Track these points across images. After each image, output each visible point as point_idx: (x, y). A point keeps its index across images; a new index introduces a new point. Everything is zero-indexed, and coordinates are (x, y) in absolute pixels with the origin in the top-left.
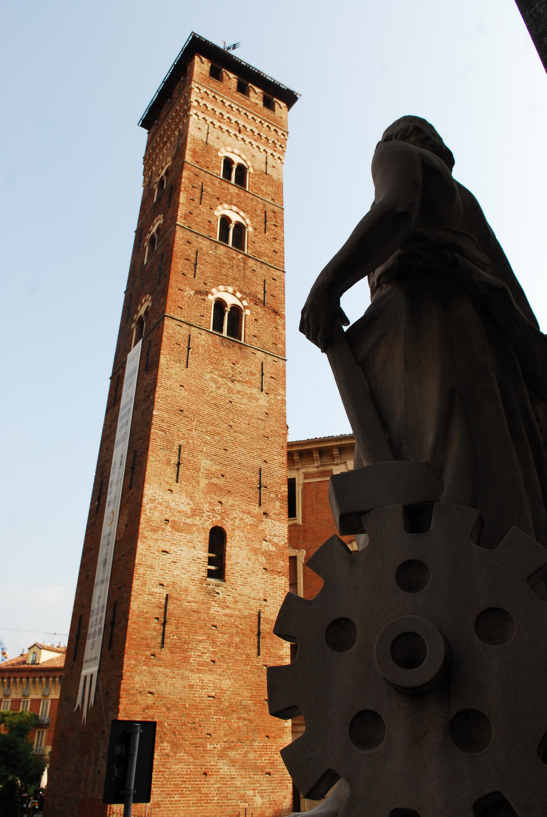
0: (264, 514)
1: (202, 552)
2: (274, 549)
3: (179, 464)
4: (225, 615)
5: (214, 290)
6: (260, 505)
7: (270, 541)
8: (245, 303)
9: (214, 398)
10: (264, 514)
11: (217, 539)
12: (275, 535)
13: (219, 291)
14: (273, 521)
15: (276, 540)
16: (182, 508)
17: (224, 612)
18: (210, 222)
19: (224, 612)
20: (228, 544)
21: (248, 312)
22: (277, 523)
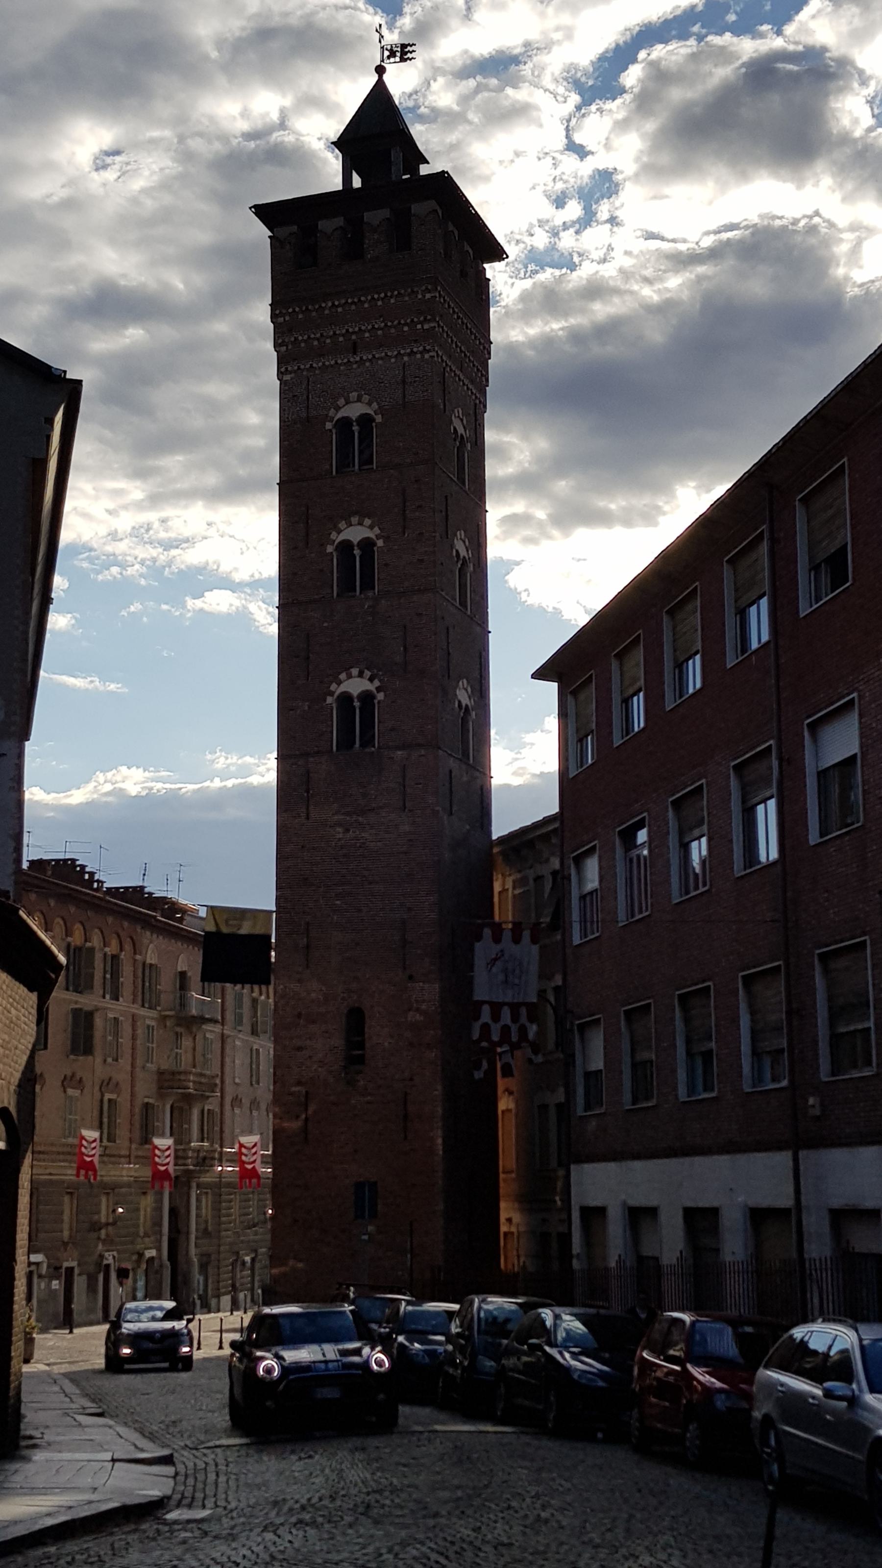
0: (411, 977)
1: (338, 1041)
2: (422, 1018)
3: (308, 947)
4: (369, 1103)
5: (333, 687)
6: (405, 968)
7: (418, 1010)
8: (377, 683)
9: (342, 847)
10: (411, 977)
11: (356, 1021)
12: (424, 1001)
13: (339, 683)
14: (421, 984)
15: (424, 1007)
16: (313, 995)
17: (366, 1099)
18: (321, 571)
19: (366, 1099)
20: (366, 1026)
21: (380, 696)
22: (426, 986)
